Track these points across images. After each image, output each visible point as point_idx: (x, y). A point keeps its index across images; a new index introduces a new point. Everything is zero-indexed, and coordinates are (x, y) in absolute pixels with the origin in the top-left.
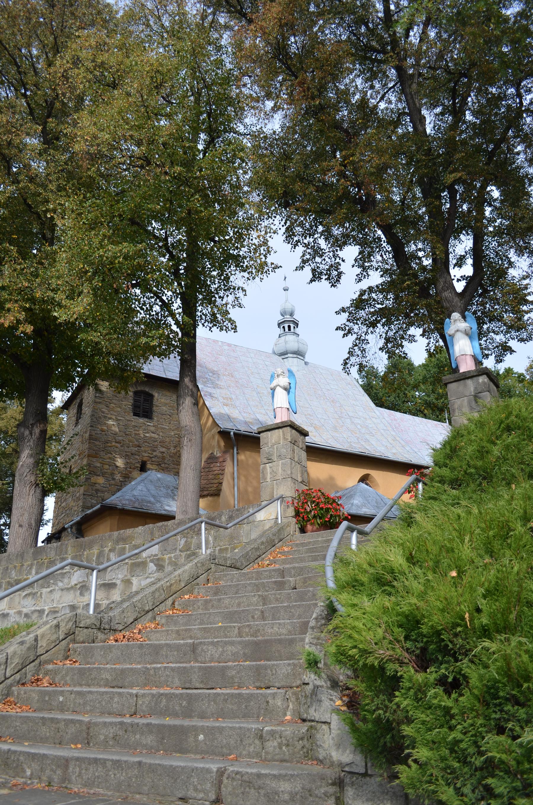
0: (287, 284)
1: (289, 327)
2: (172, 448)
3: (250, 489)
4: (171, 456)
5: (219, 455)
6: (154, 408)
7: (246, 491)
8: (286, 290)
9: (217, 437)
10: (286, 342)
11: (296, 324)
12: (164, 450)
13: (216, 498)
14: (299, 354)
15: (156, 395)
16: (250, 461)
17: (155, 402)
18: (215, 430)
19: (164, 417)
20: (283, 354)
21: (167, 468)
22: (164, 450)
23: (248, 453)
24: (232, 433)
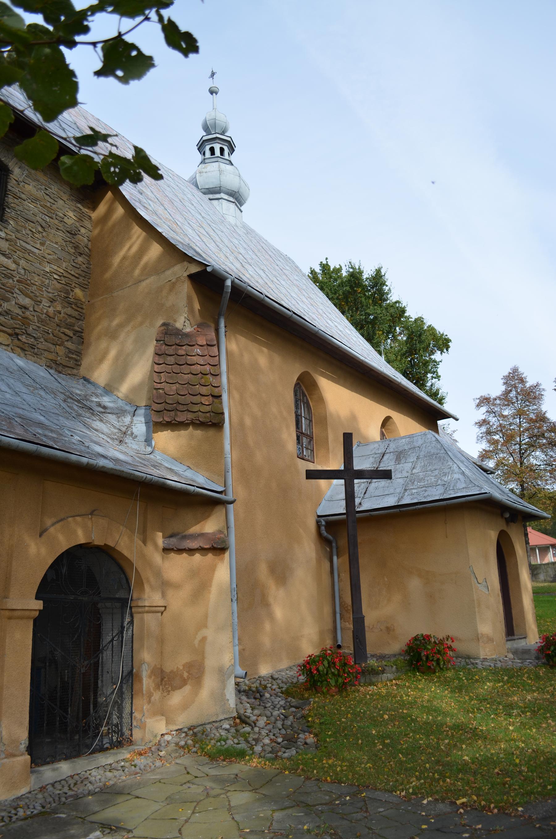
0: (216, 83)
1: (222, 150)
2: (45, 303)
3: (248, 421)
4: (41, 321)
5: (188, 330)
6: (10, 199)
7: (242, 423)
8: (212, 92)
9: (186, 287)
10: (221, 172)
11: (232, 150)
12: (27, 301)
13: (211, 432)
14: (237, 198)
15: (17, 172)
16: (246, 358)
17: (12, 185)
18: (182, 271)
19: (30, 225)
20: (213, 192)
21: (32, 347)
22: (27, 301)
23: (242, 340)
24: (229, 283)
